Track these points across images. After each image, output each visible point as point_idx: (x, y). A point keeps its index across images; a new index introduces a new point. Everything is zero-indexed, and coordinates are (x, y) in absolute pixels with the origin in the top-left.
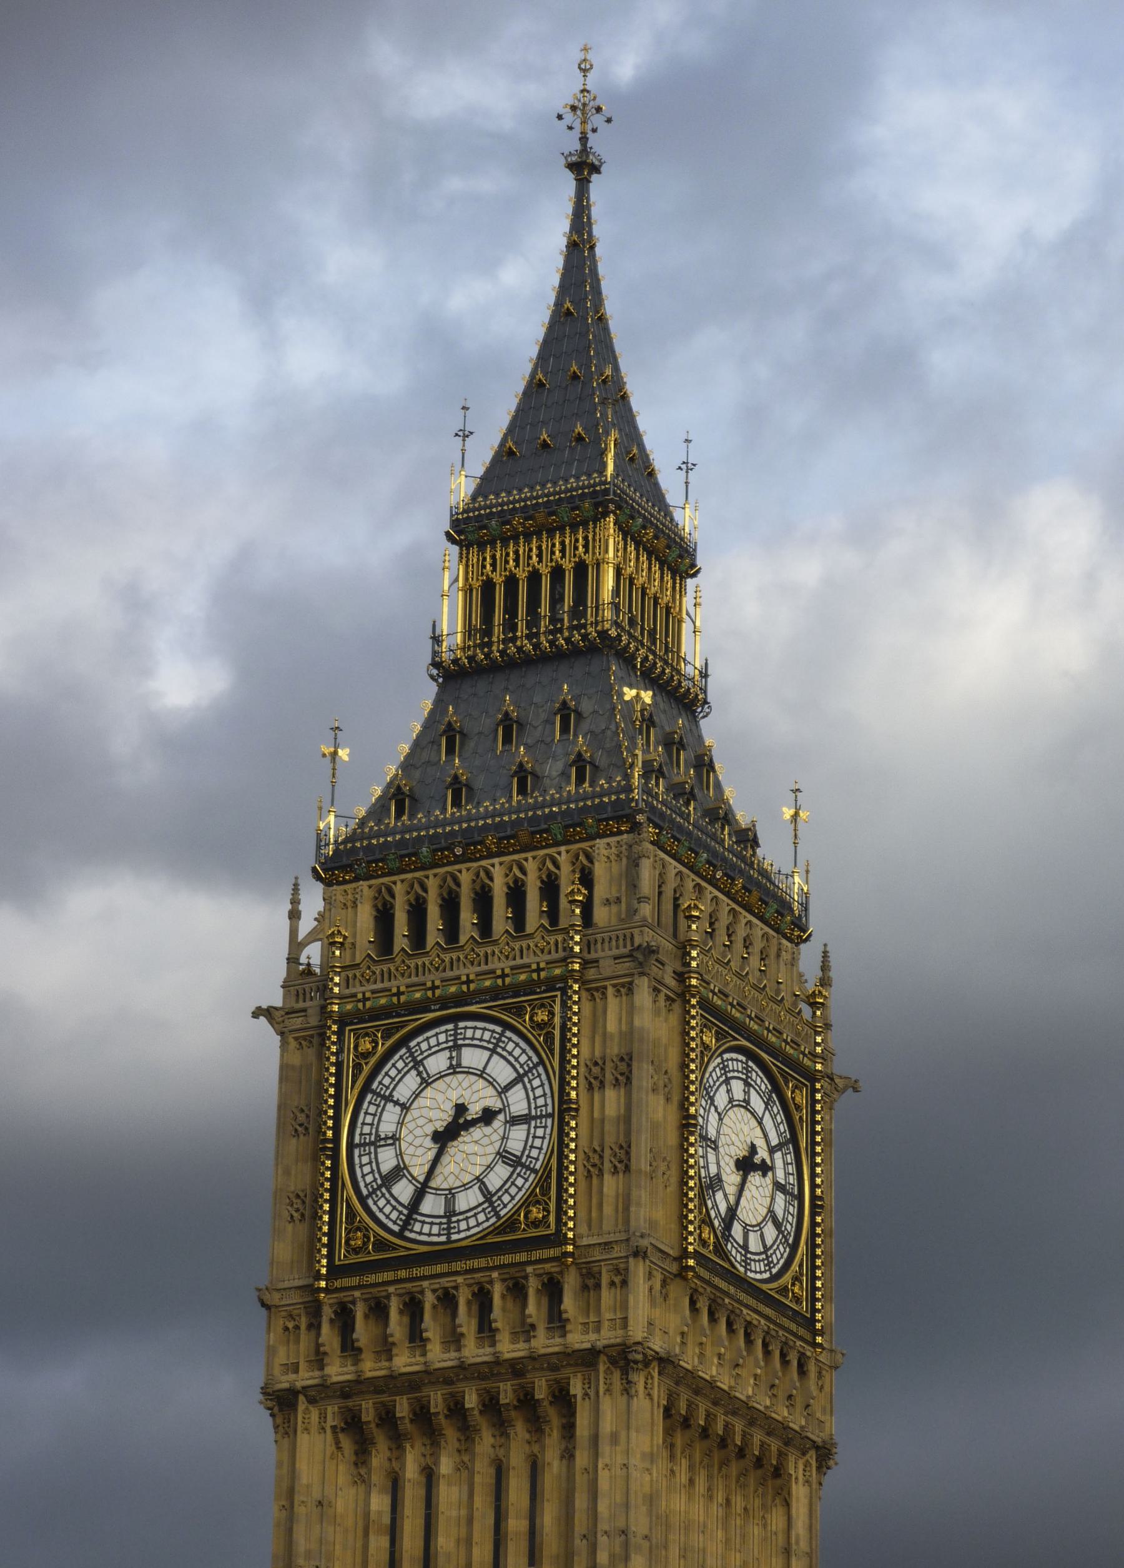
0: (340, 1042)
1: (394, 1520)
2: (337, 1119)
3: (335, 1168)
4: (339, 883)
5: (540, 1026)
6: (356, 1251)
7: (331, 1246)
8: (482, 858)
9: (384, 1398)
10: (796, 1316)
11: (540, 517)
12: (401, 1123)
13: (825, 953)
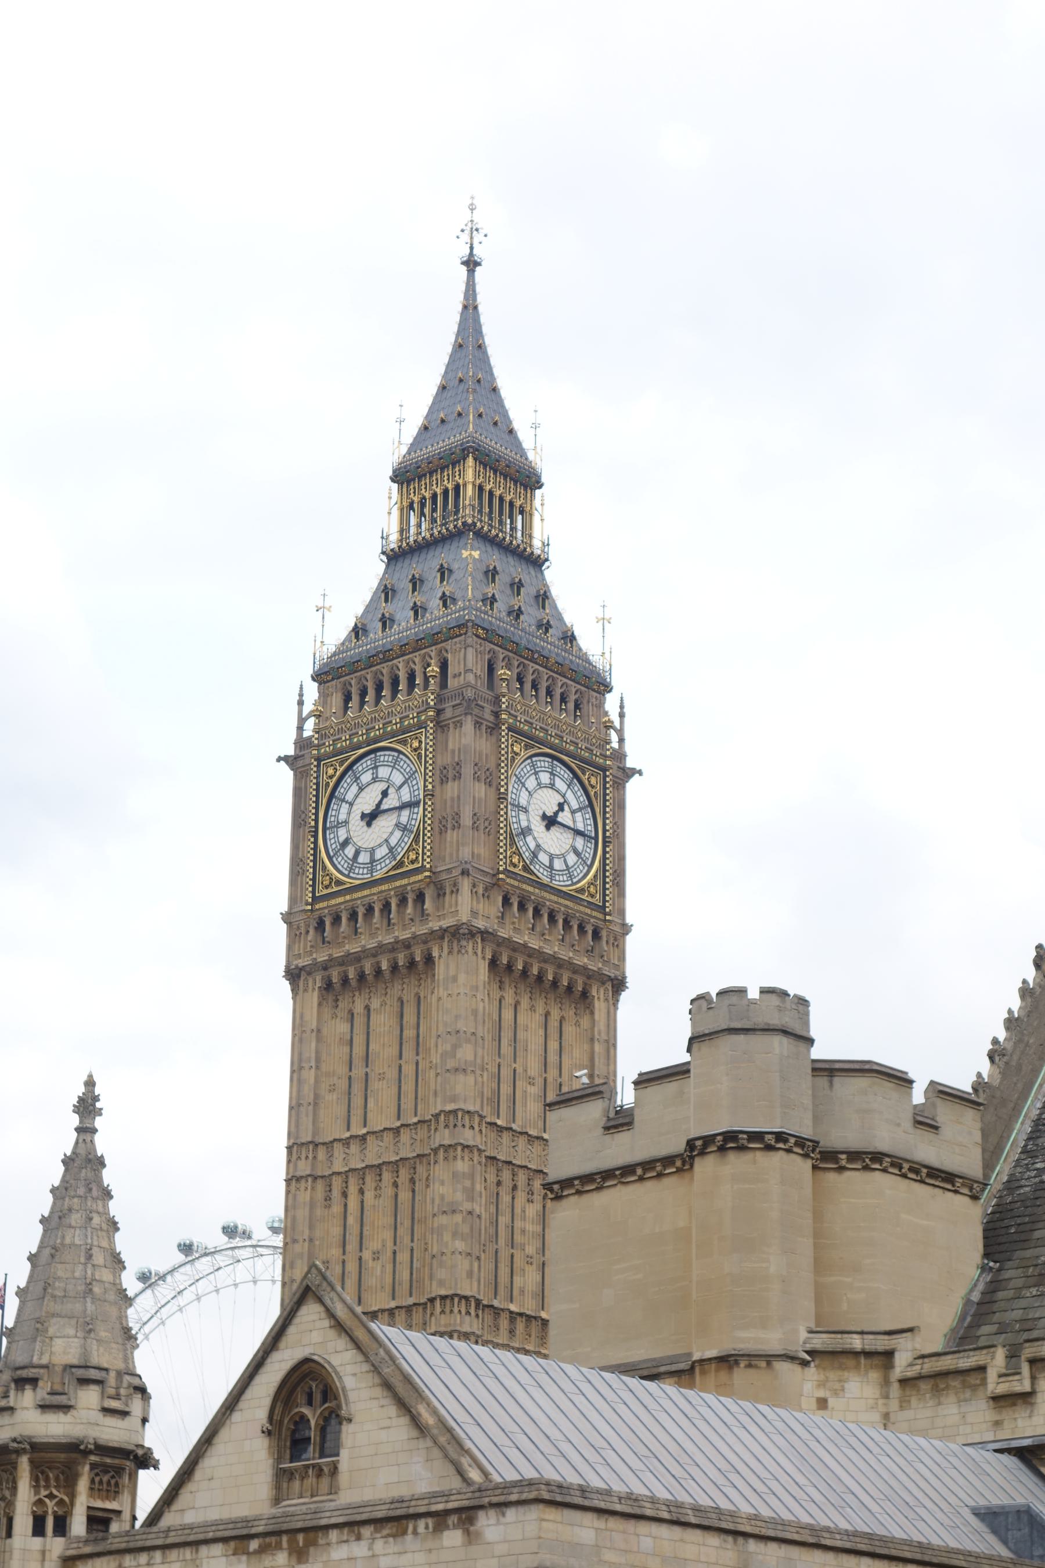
0: (318, 772)
2: (316, 814)
3: (316, 843)
4: (325, 683)
5: (415, 750)
6: (327, 887)
7: (313, 886)
8: (393, 659)
9: (344, 968)
12: (349, 813)
13: (622, 700)
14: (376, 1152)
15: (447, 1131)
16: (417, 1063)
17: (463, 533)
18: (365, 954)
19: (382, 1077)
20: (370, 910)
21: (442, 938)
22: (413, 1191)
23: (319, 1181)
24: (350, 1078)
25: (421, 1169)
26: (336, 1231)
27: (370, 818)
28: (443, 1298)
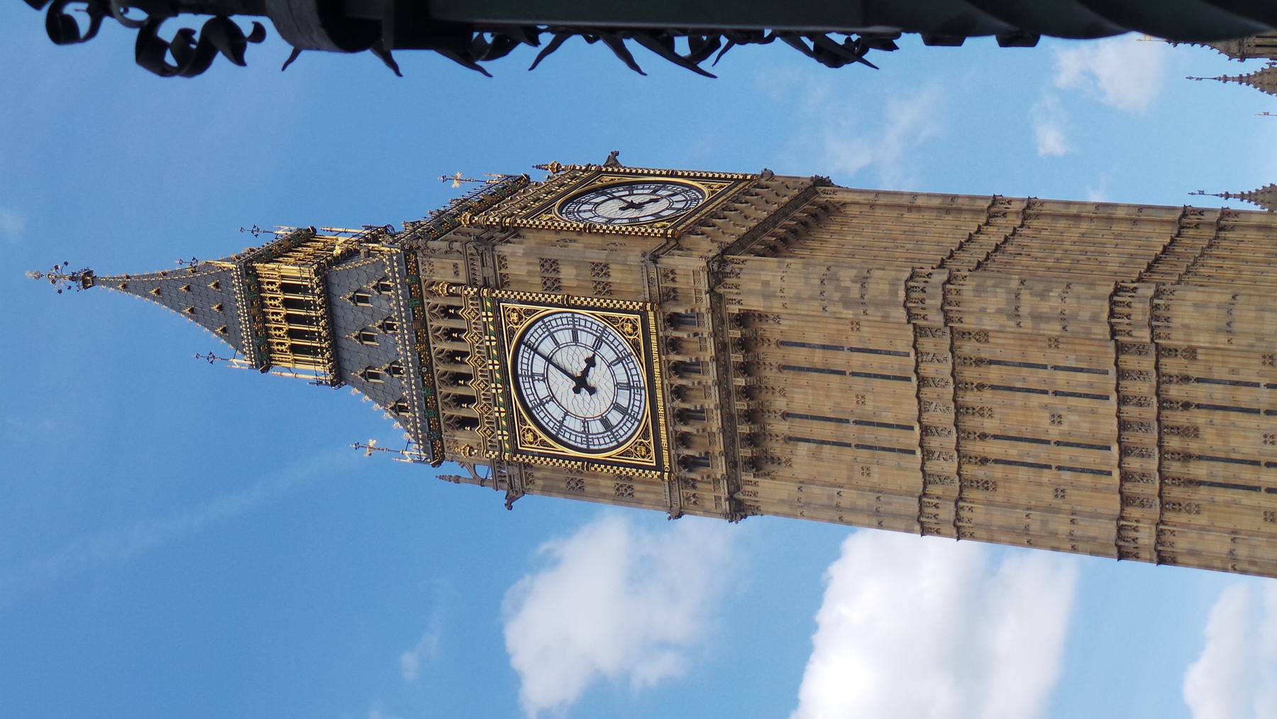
1: (814, 441)
2: (571, 458)
3: (599, 462)
4: (443, 451)
5: (520, 318)
6: (648, 451)
8: (430, 355)
10: (730, 188)
11: (254, 311)
12: (576, 417)
14: (942, 417)
15: (928, 302)
16: (852, 350)
17: (326, 276)
18: (724, 405)
19: (861, 399)
20: (679, 392)
21: (720, 297)
22: (991, 362)
23: (966, 494)
24: (857, 446)
25: (968, 347)
26: (1023, 473)
27: (581, 383)
28: (1112, 314)
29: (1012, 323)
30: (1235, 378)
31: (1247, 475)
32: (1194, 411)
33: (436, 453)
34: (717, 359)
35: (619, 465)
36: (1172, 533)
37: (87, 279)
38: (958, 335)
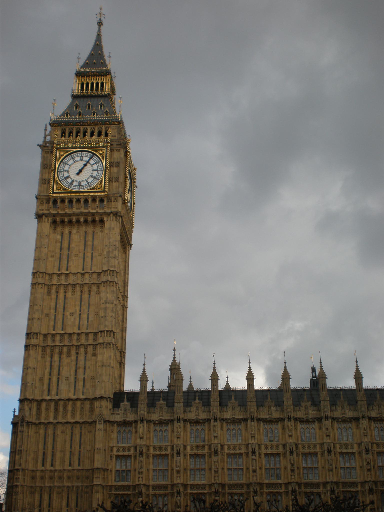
3: (54, 174)
5: (101, 154)
6: (59, 190)
9: (62, 217)
11: (95, 73)
14: (71, 280)
18: (74, 214)
19: (76, 255)
21: (109, 215)
22: (90, 295)
24: (61, 254)
25: (94, 288)
26: (53, 304)
28: (107, 331)
29: (103, 302)
30: (87, 368)
31: (55, 372)
32: (75, 356)
33: (54, 124)
34: (89, 213)
35: (54, 180)
36: (36, 350)
37: (100, 24)
38: (98, 285)
